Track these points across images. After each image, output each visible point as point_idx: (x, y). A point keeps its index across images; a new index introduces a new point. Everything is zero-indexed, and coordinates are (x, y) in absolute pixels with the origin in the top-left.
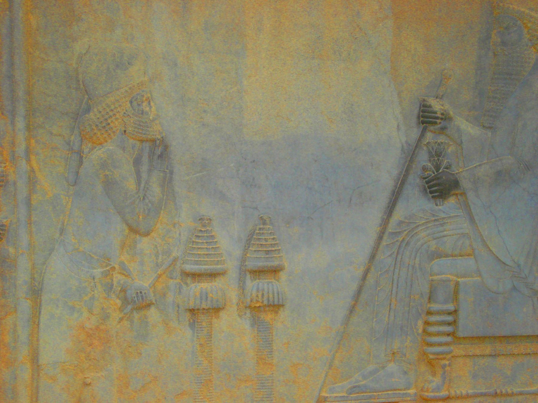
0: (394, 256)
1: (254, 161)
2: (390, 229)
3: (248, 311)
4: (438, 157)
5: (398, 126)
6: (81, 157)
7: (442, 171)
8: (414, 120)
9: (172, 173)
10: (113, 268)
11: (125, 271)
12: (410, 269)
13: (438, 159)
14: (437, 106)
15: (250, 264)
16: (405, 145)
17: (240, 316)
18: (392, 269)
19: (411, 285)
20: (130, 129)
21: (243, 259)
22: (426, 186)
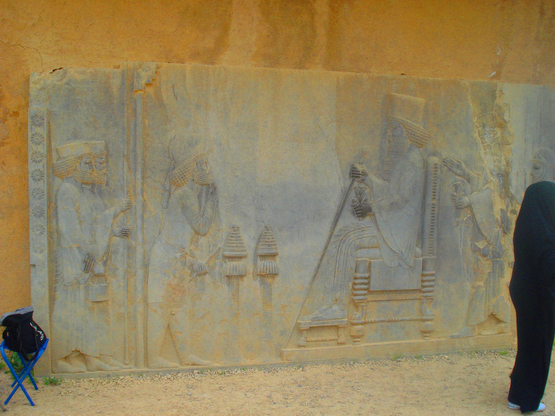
1: (262, 196)
2: (335, 234)
5: (339, 178)
6: (170, 194)
8: (348, 176)
9: (218, 202)
10: (186, 253)
11: (193, 255)
13: (361, 196)
14: (360, 168)
15: (260, 252)
16: (343, 188)
17: (254, 280)
19: (346, 263)
20: (196, 179)
21: (256, 249)
22: (354, 210)
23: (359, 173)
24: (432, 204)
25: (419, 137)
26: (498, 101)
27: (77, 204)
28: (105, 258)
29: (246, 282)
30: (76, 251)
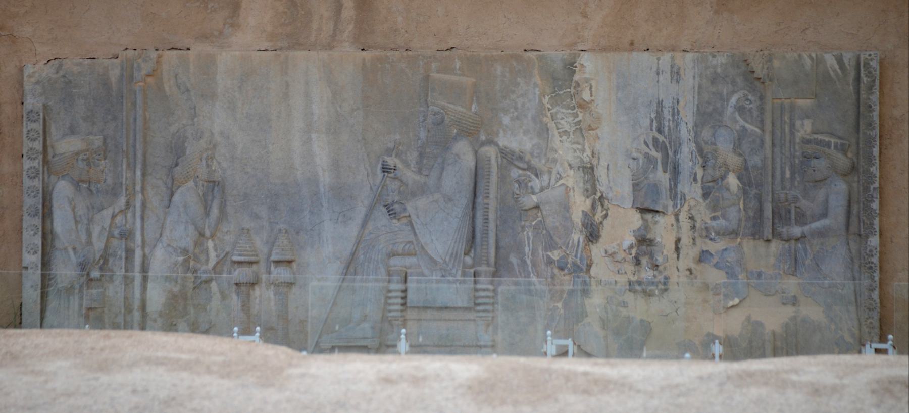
3: (272, 287)
15: (274, 258)
17: (267, 289)
25: (465, 124)
26: (576, 77)
27: (73, 203)
28: (101, 261)
29: (257, 292)
30: (71, 253)
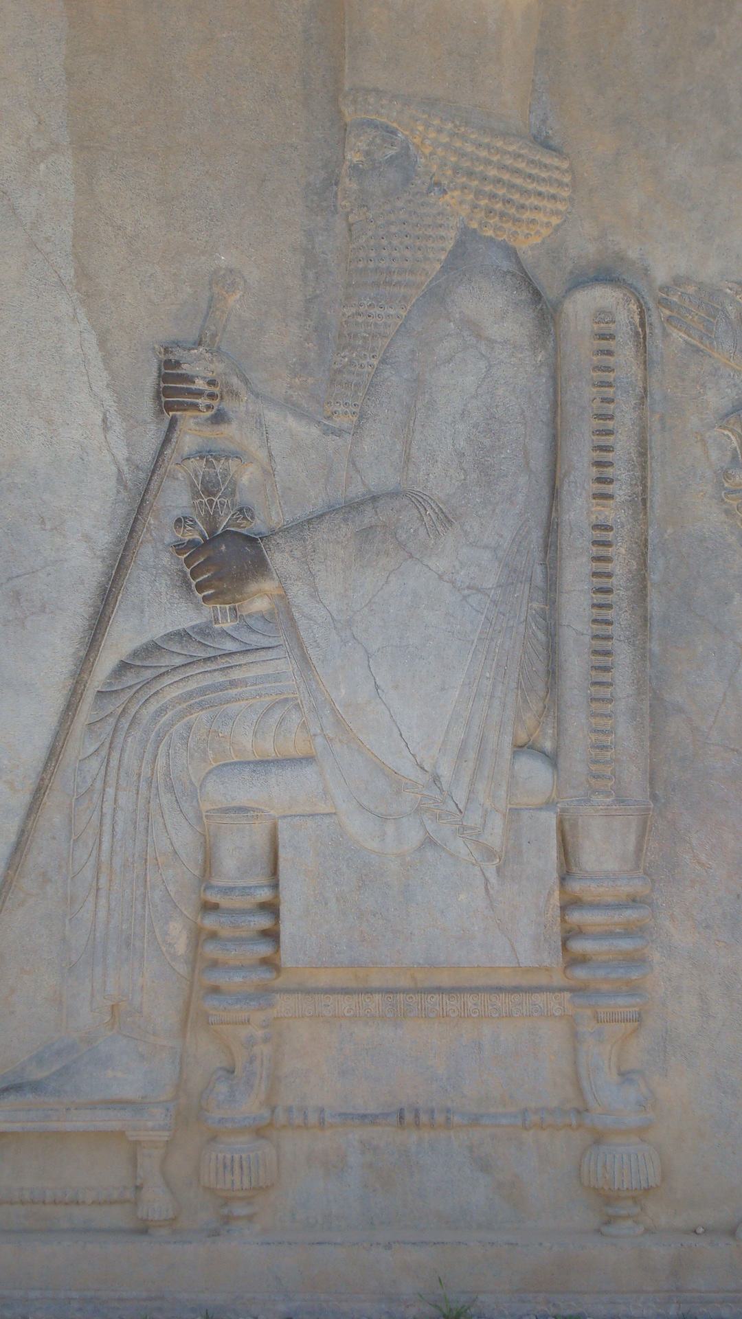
0: (104, 753)
4: (209, 496)
5: (104, 420)
7: (221, 534)
8: (146, 405)
12: (143, 785)
13: (211, 502)
14: (199, 367)
16: (126, 469)
18: (99, 785)
19: (147, 829)
23: (193, 387)
24: (596, 527)
